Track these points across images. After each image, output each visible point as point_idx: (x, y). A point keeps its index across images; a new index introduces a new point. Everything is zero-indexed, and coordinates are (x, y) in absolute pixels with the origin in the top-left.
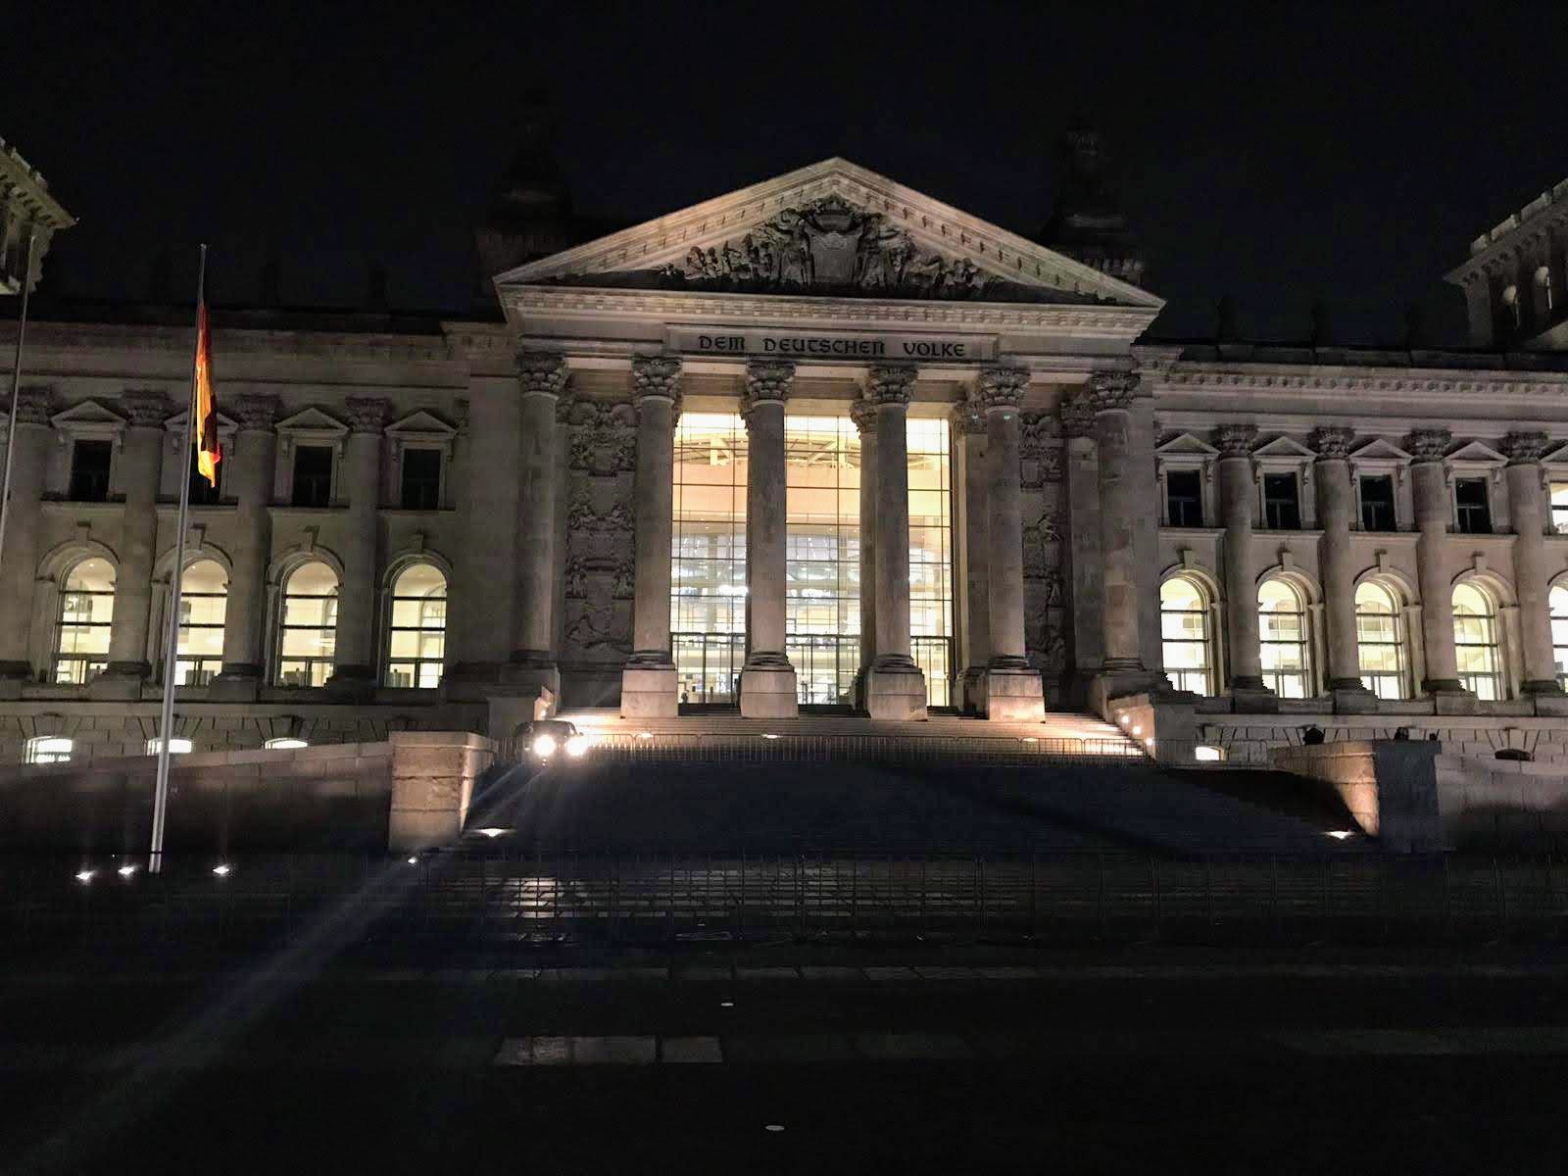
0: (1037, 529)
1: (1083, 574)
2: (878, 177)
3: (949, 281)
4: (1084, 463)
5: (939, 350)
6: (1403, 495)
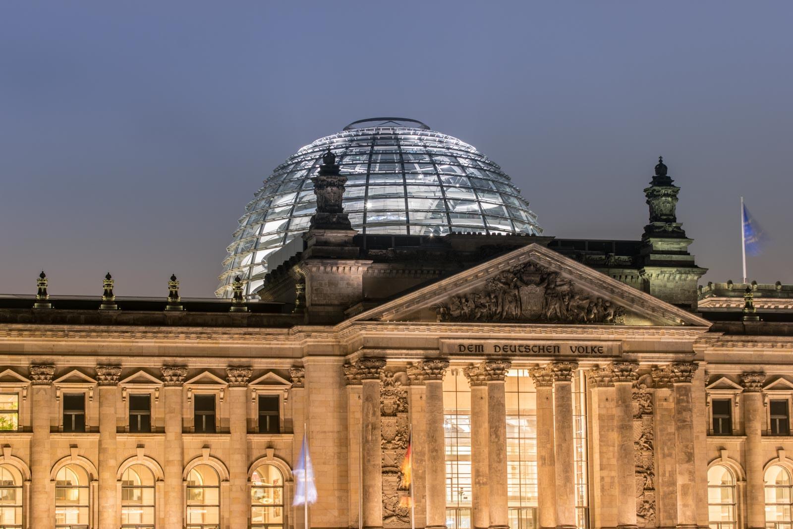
1: (665, 471)
4: (665, 403)
5: (589, 350)
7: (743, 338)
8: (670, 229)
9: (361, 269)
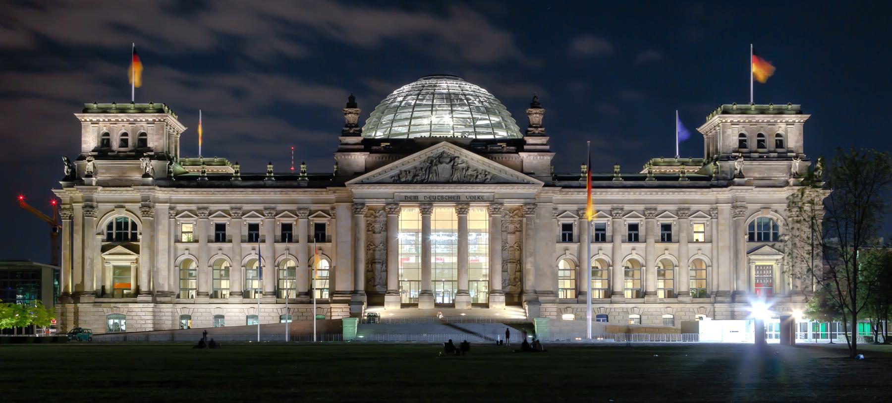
0: (513, 247)
3: (480, 177)
5: (477, 198)
6: (642, 231)
8: (537, 132)
9: (363, 157)
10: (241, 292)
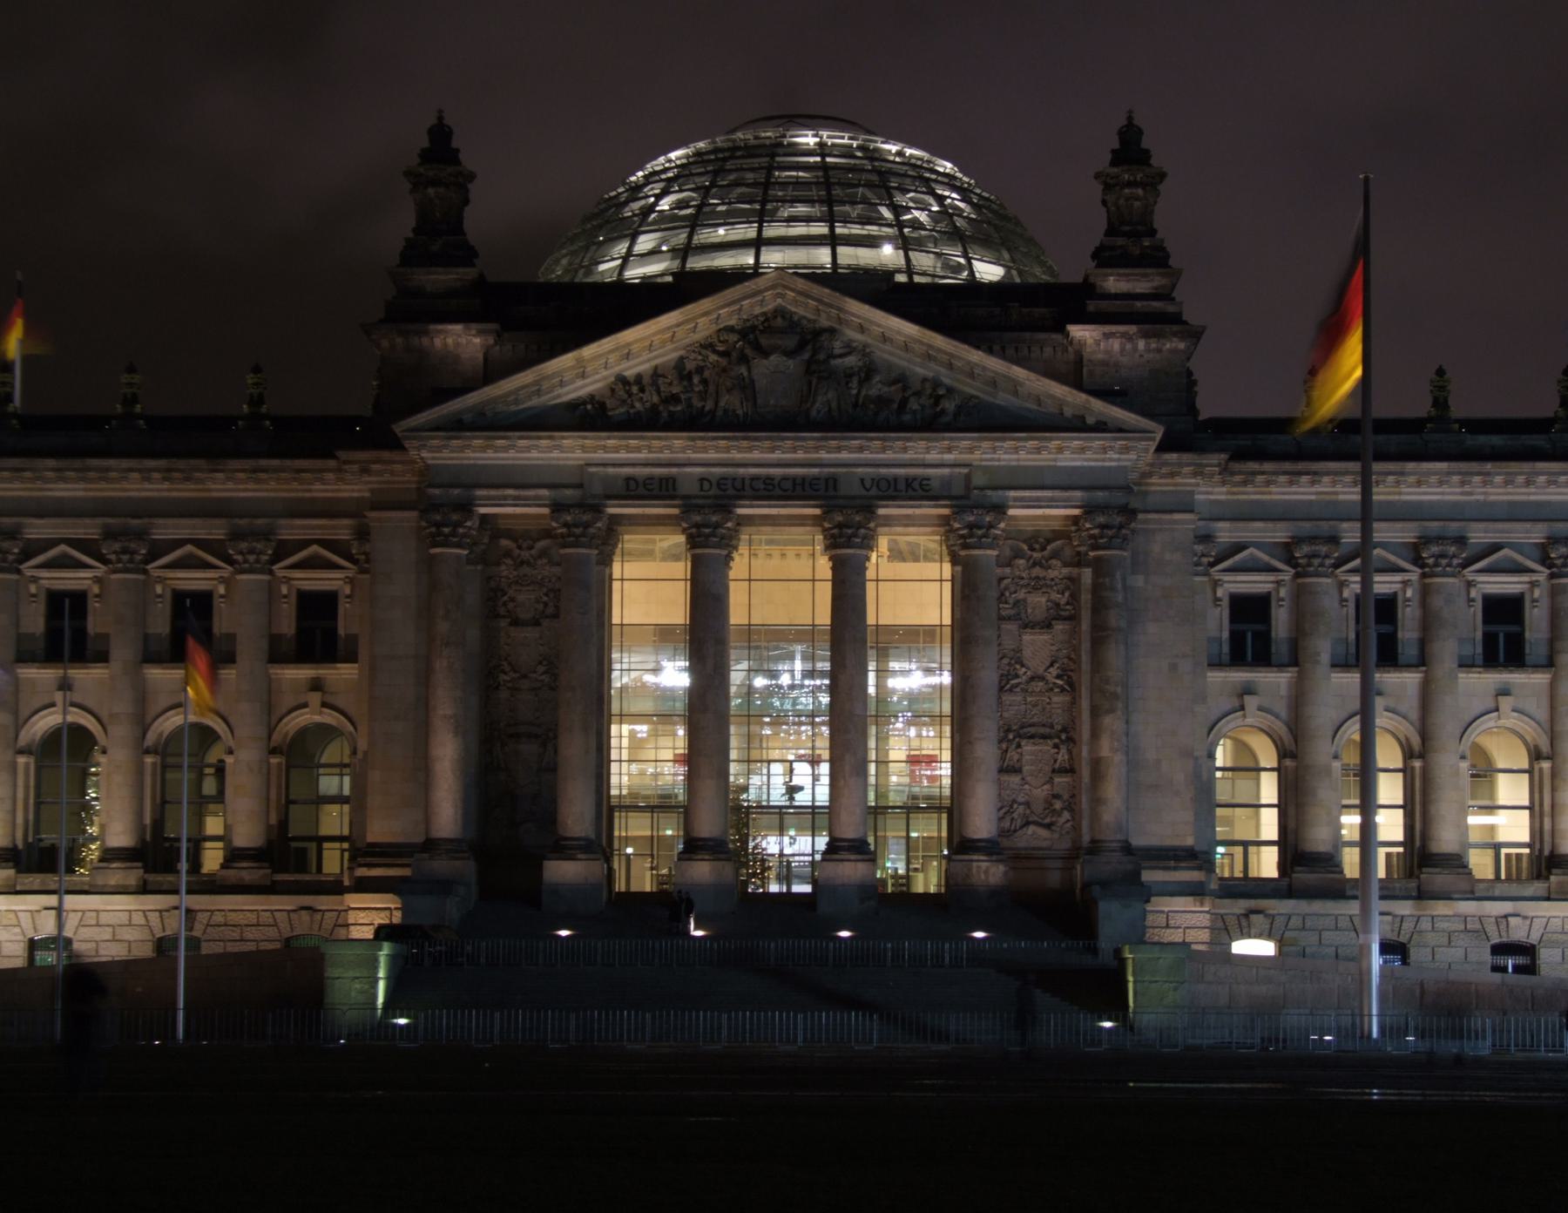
0: (1042, 678)
2: (827, 291)
3: (914, 405)
5: (902, 486)
7: (1287, 466)
9: (477, 340)
10: (15, 847)
